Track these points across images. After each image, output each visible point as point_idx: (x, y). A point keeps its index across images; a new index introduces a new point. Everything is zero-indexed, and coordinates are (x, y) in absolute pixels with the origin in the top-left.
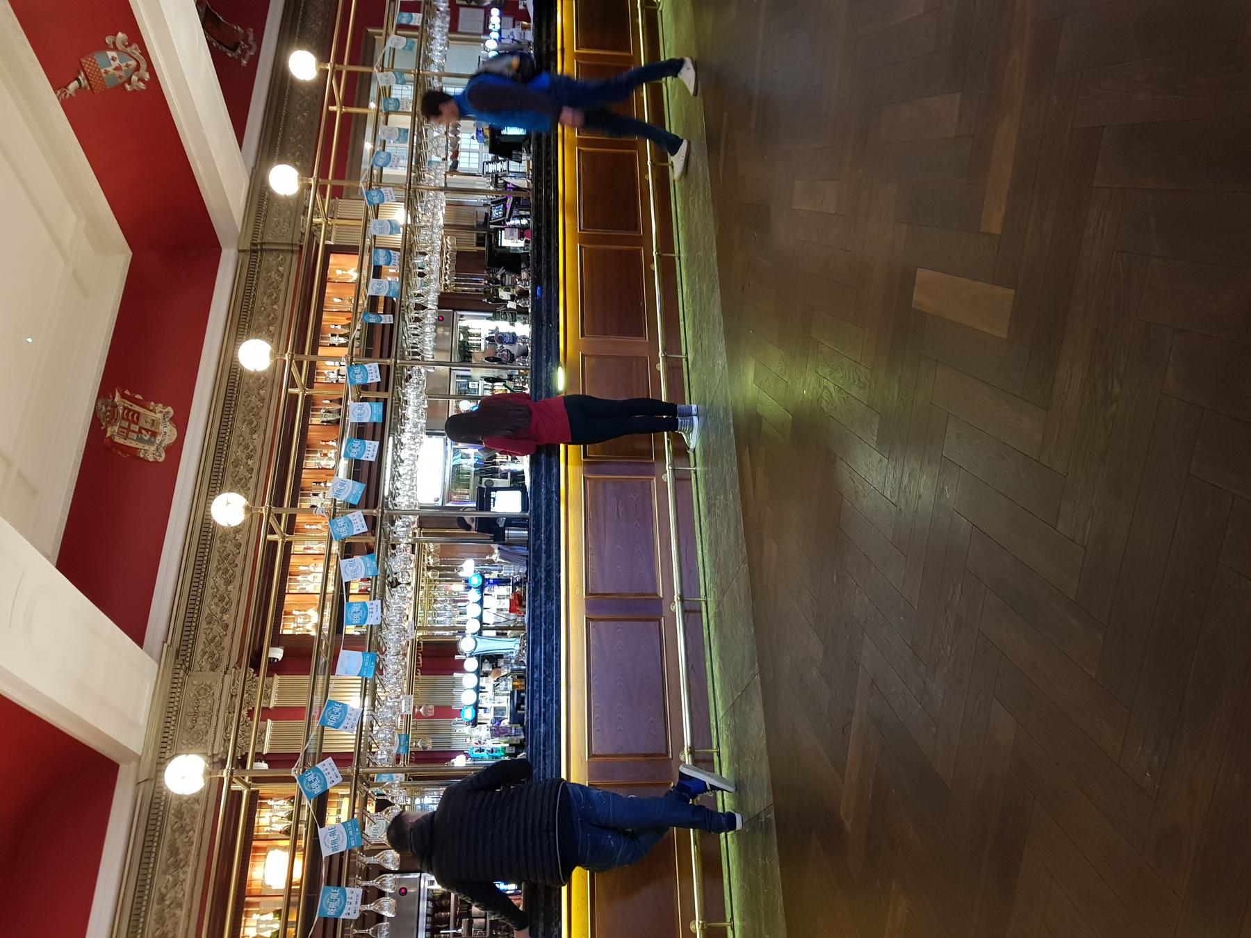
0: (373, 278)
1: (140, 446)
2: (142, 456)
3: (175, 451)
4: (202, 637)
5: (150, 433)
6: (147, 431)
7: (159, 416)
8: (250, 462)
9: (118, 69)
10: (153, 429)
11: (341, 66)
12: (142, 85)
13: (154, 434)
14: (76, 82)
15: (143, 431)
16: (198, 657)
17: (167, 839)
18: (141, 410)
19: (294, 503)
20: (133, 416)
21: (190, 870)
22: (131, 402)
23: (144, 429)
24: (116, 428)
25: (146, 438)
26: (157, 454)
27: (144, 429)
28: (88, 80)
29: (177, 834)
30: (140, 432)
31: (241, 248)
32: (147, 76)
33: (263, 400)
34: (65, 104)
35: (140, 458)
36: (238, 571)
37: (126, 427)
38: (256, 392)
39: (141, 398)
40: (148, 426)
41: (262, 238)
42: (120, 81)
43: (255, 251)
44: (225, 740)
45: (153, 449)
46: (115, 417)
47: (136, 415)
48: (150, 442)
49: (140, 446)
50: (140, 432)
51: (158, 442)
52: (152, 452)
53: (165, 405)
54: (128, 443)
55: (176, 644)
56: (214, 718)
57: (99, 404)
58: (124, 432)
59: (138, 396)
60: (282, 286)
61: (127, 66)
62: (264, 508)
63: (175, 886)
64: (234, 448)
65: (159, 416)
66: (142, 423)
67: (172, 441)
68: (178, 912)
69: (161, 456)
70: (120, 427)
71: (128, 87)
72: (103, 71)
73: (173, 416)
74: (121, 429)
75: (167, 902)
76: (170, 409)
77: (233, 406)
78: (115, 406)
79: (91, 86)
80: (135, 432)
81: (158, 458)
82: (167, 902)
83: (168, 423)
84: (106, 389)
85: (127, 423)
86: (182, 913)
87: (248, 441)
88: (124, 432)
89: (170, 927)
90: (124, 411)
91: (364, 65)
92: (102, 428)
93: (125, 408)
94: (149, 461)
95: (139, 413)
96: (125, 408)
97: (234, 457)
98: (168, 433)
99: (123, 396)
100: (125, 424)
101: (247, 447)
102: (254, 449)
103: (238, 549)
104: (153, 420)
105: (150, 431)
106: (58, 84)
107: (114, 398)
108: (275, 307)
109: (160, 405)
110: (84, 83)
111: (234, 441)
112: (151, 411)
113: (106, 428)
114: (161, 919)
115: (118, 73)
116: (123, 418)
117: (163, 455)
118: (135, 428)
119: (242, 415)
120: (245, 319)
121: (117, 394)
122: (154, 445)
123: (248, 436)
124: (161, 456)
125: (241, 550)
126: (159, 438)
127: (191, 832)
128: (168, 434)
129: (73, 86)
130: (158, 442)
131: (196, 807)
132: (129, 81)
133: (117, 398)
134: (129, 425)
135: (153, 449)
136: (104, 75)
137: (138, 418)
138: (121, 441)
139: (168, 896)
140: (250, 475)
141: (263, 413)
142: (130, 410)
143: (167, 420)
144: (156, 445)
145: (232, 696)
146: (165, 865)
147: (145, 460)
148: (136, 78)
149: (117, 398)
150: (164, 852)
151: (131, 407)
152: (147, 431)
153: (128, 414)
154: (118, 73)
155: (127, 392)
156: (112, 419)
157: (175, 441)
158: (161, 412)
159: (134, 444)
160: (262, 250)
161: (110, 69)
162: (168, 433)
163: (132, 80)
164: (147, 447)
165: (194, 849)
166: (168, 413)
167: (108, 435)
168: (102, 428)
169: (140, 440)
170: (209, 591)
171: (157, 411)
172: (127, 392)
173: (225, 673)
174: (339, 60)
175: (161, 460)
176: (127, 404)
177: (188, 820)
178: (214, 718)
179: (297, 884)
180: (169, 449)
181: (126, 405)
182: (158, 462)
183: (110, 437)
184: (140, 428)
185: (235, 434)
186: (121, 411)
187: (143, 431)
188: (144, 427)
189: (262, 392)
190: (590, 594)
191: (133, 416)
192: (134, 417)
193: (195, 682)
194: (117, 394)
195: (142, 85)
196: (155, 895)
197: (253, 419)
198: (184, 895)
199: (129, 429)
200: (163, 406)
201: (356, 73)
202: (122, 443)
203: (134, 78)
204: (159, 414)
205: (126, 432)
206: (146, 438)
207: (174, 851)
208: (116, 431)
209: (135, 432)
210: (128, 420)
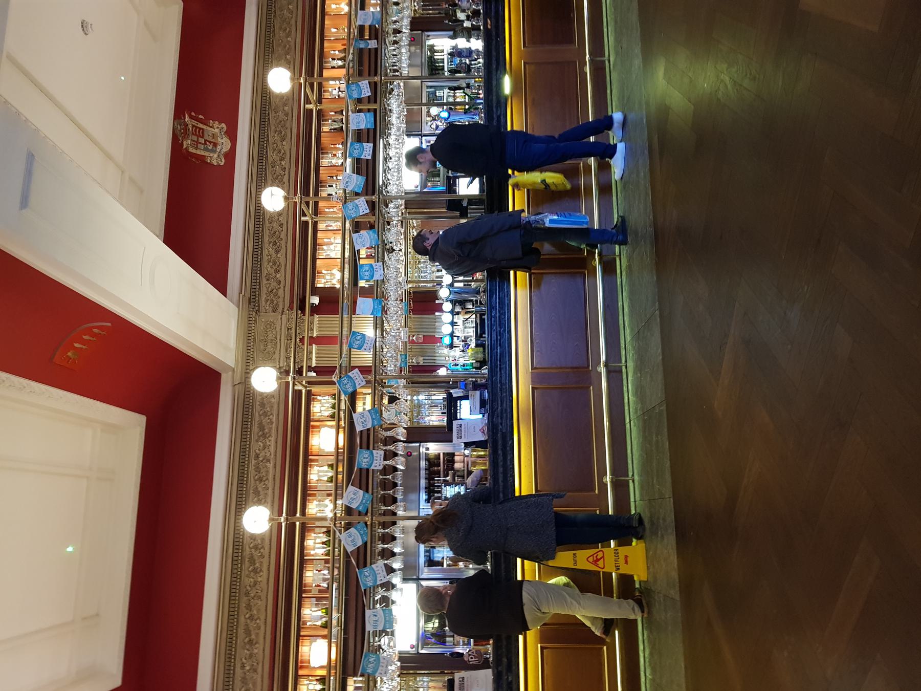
0: (360, 10)
1: (206, 154)
2: (209, 161)
3: (231, 156)
4: (264, 290)
6: (210, 142)
7: (217, 131)
8: (283, 163)
13: (215, 145)
15: (208, 143)
16: (263, 303)
19: (316, 194)
20: (199, 132)
21: (273, 439)
24: (189, 142)
25: (210, 148)
27: (207, 141)
30: (205, 144)
33: (287, 115)
36: (283, 243)
38: (281, 109)
40: (210, 139)
44: (287, 358)
45: (216, 156)
46: (188, 133)
47: (201, 131)
48: (215, 152)
49: (206, 154)
50: (205, 144)
51: (218, 150)
52: (215, 159)
53: (220, 123)
54: (198, 152)
55: (248, 295)
56: (278, 343)
57: (176, 124)
58: (194, 144)
59: (200, 117)
60: (293, 21)
62: (297, 197)
63: (265, 449)
64: (270, 152)
65: (217, 131)
66: (206, 137)
67: (228, 149)
68: (268, 465)
70: (192, 140)
73: (227, 130)
74: (192, 142)
76: (223, 125)
78: (186, 125)
80: (202, 144)
82: (261, 459)
83: (224, 136)
84: (178, 114)
86: (270, 466)
88: (194, 144)
89: (264, 474)
92: (180, 142)
93: (193, 126)
95: (203, 129)
96: (193, 126)
97: (271, 160)
98: (224, 144)
99: (191, 117)
100: (195, 138)
101: (280, 151)
104: (213, 134)
105: (212, 142)
107: (185, 118)
109: (217, 122)
112: (211, 127)
113: (182, 142)
114: (258, 469)
117: (223, 160)
119: (273, 128)
120: (269, 50)
123: (279, 143)
125: (283, 228)
126: (219, 147)
127: (271, 416)
128: (224, 143)
130: (218, 150)
131: (273, 400)
135: (216, 156)
138: (194, 151)
139: (261, 455)
141: (288, 124)
142: (197, 127)
145: (288, 329)
146: (257, 436)
147: (211, 164)
150: (255, 429)
151: (196, 125)
152: (210, 142)
153: (195, 131)
155: (193, 114)
156: (186, 135)
157: (230, 149)
158: (218, 128)
159: (202, 153)
162: (224, 144)
165: (274, 425)
166: (222, 128)
167: (185, 147)
168: (180, 142)
169: (206, 149)
170: (265, 258)
172: (193, 114)
173: (282, 314)
175: (222, 164)
176: (195, 123)
177: (268, 408)
178: (278, 343)
179: (341, 449)
181: (194, 124)
182: (220, 165)
183: (186, 148)
184: (205, 140)
185: (270, 142)
187: (208, 143)
188: (208, 139)
189: (286, 108)
191: (199, 132)
192: (200, 133)
193: (263, 320)
196: (253, 454)
197: (282, 130)
198: (271, 455)
199: (198, 142)
200: (219, 123)
202: (195, 152)
204: (216, 129)
205: (196, 144)
206: (210, 148)
207: (261, 427)
208: (190, 144)
209: (202, 144)
210: (196, 135)
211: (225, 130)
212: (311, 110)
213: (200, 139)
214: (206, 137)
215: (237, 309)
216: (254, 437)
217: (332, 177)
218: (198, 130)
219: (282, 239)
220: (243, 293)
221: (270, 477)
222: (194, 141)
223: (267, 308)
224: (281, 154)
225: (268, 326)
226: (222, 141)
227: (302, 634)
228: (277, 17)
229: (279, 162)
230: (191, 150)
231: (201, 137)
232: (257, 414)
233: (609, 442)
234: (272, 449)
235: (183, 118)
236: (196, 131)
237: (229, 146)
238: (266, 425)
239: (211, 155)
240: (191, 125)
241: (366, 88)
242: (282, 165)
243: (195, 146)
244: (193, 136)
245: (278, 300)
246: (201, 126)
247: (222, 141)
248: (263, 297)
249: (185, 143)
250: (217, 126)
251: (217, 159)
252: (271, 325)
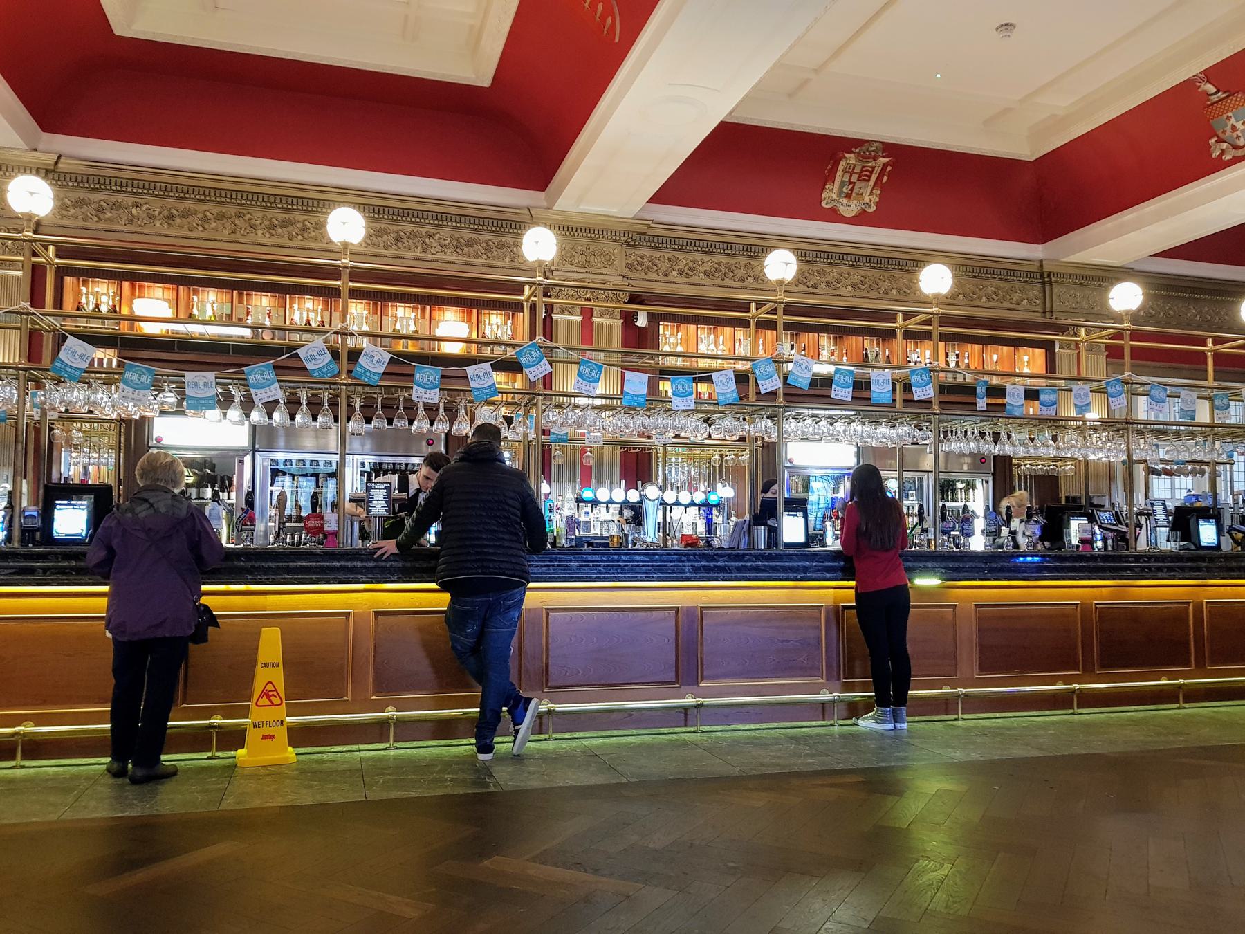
1: (837, 184)
2: (827, 187)
3: (833, 216)
4: (656, 254)
6: (852, 190)
7: (867, 199)
8: (823, 285)
9: (1234, 128)
10: (854, 195)
11: (1128, 337)
12: (1216, 154)
13: (848, 196)
14: (1215, 90)
15: (851, 186)
16: (639, 252)
17: (481, 237)
20: (866, 175)
21: (454, 258)
23: (853, 187)
24: (853, 162)
25: (845, 190)
27: (853, 187)
28: (1217, 102)
29: (394, 235)
30: (850, 183)
31: (1044, 262)
32: (1227, 157)
34: (1187, 87)
35: (824, 188)
36: (719, 282)
40: (856, 190)
41: (1057, 282)
42: (1220, 133)
43: (1042, 276)
45: (834, 196)
48: (839, 195)
49: (837, 184)
50: (850, 183)
51: (841, 200)
52: (830, 195)
53: (877, 204)
54: (839, 173)
55: (650, 232)
57: (877, 144)
59: (885, 178)
60: (728, 282)
61: (1238, 137)
64: (837, 269)
65: (867, 199)
66: (858, 185)
68: (419, 250)
70: (855, 165)
71: (1214, 140)
72: (1230, 114)
75: (134, 211)
76: (874, 208)
79: (1211, 105)
83: (859, 208)
84: (890, 148)
86: (418, 253)
89: (312, 234)
91: (1215, 371)
92: (853, 150)
93: (873, 168)
95: (869, 180)
96: (873, 168)
98: (849, 208)
99: (885, 166)
100: (858, 169)
101: (838, 281)
102: (836, 288)
104: (862, 194)
106: (1209, 74)
107: (884, 157)
108: (984, 298)
109: (877, 199)
110: (1214, 98)
111: (844, 269)
112: (871, 191)
113: (852, 152)
115: (1229, 129)
116: (863, 167)
117: (828, 206)
121: (887, 160)
126: (845, 201)
127: (396, 247)
129: (1211, 88)
130: (841, 200)
132: (1220, 141)
133: (883, 160)
134: (857, 173)
135: (834, 196)
136: (1225, 116)
137: (864, 180)
138: (841, 167)
139: (433, 241)
141: (874, 294)
142: (871, 172)
143: (863, 206)
148: (1224, 147)
149: (883, 160)
150: (469, 235)
152: (852, 190)
153: (867, 171)
154: (1229, 129)
155: (889, 168)
156: (862, 158)
158: (871, 201)
159: (838, 179)
160: (1043, 283)
161: (1233, 121)
162: (849, 208)
163: (1222, 144)
166: (870, 207)
167: (847, 155)
168: (853, 150)
169: (842, 184)
170: (698, 257)
172: (889, 168)
173: (624, 277)
174: (1135, 336)
175: (823, 204)
176: (878, 170)
183: (845, 157)
184: (854, 184)
186: (870, 164)
187: (851, 186)
189: (894, 292)
190: (548, 614)
191: (866, 175)
192: (864, 176)
193: (616, 251)
194: (887, 160)
195: (1216, 154)
196: (139, 199)
199: (852, 173)
201: (1205, 363)
203: (1224, 146)
204: (869, 198)
206: (845, 190)
207: (470, 243)
210: (862, 171)
211: (866, 210)
212: (748, 310)
213: (857, 176)
214: (858, 185)
215: (631, 216)
216: (457, 233)
217: (804, 350)
218: (868, 174)
220: (652, 225)
221: (401, 253)
222: (853, 169)
224: (835, 283)
226: (853, 206)
227: (126, 284)
228: (1012, 284)
229: (824, 280)
230: (842, 165)
231: (859, 177)
232: (489, 238)
233: (409, 716)
234: (440, 256)
236: (866, 171)
238: (474, 249)
239: (835, 191)
241: (842, 394)
244: (860, 167)
246: (874, 178)
247: (853, 206)
248: (647, 253)
249: (852, 155)
250: (873, 199)
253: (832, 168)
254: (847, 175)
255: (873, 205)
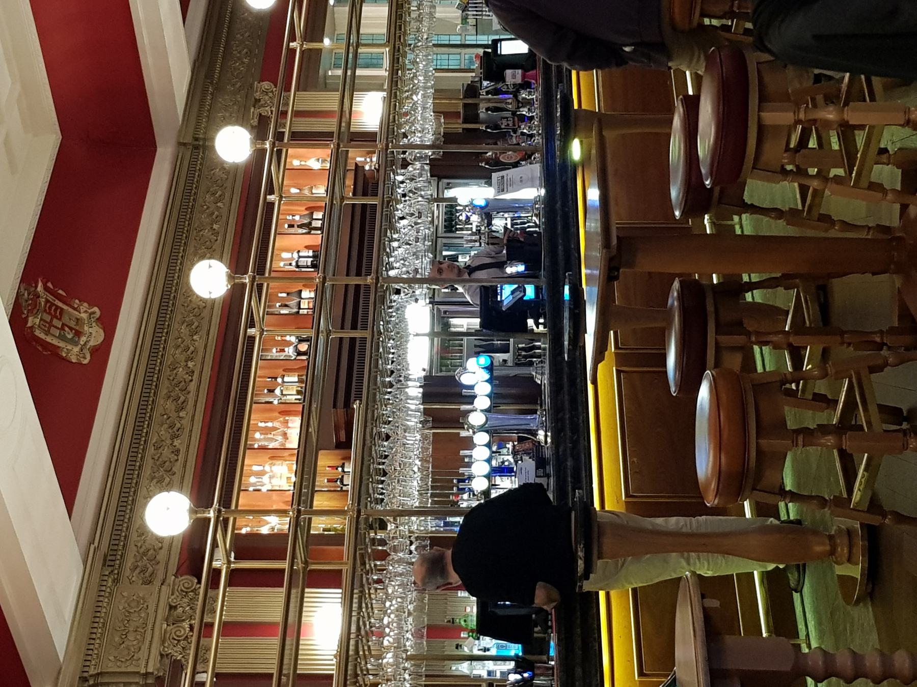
1: (62, 344)
2: (64, 355)
5: (74, 331)
6: (71, 329)
10: (77, 328)
13: (78, 334)
15: (67, 329)
18: (65, 307)
22: (55, 297)
25: (70, 336)
26: (81, 355)
30: (62, 329)
37: (49, 321)
39: (64, 294)
40: (72, 324)
45: (76, 349)
46: (38, 308)
48: (74, 343)
49: (62, 344)
50: (62, 329)
51: (82, 343)
54: (49, 339)
64: (171, 350)
66: (66, 319)
69: (85, 358)
70: (41, 319)
73: (100, 317)
74: (42, 322)
77: (185, 231)
81: (82, 359)
85: (50, 317)
87: (188, 341)
90: (46, 305)
94: (72, 362)
95: (62, 309)
96: (47, 301)
98: (95, 335)
99: (46, 288)
100: (48, 318)
103: (177, 456)
104: (78, 319)
105: (73, 329)
118: (56, 322)
121: (40, 285)
122: (77, 345)
124: (85, 358)
126: (83, 339)
135: (76, 349)
137: (61, 314)
140: (176, 457)
144: (80, 346)
147: (66, 360)
152: (71, 329)
155: (50, 285)
157: (102, 342)
159: (55, 342)
162: (95, 335)
164: (69, 347)
169: (62, 338)
171: (82, 311)
172: (50, 285)
175: (86, 362)
176: (51, 298)
178: (149, 632)
180: (94, 351)
182: (81, 364)
184: (63, 325)
186: (43, 303)
188: (68, 324)
191: (55, 311)
194: (40, 285)
197: (180, 395)
199: (51, 324)
204: (84, 312)
205: (48, 327)
206: (70, 336)
210: (50, 313)
219: (189, 393)
223: (133, 579)
225: (133, 604)
235: (34, 285)
237: (101, 338)
240: (44, 300)
242: (189, 368)
243: (46, 329)
244: (45, 314)
245: (157, 567)
246: (60, 304)
250: (85, 309)
251: (77, 355)
252: (138, 602)
253: (42, 345)
254: (53, 330)
255: (92, 310)
